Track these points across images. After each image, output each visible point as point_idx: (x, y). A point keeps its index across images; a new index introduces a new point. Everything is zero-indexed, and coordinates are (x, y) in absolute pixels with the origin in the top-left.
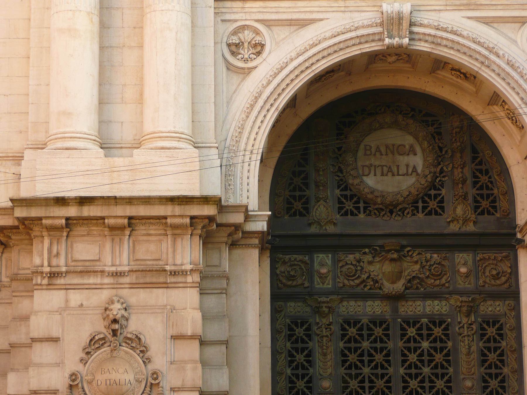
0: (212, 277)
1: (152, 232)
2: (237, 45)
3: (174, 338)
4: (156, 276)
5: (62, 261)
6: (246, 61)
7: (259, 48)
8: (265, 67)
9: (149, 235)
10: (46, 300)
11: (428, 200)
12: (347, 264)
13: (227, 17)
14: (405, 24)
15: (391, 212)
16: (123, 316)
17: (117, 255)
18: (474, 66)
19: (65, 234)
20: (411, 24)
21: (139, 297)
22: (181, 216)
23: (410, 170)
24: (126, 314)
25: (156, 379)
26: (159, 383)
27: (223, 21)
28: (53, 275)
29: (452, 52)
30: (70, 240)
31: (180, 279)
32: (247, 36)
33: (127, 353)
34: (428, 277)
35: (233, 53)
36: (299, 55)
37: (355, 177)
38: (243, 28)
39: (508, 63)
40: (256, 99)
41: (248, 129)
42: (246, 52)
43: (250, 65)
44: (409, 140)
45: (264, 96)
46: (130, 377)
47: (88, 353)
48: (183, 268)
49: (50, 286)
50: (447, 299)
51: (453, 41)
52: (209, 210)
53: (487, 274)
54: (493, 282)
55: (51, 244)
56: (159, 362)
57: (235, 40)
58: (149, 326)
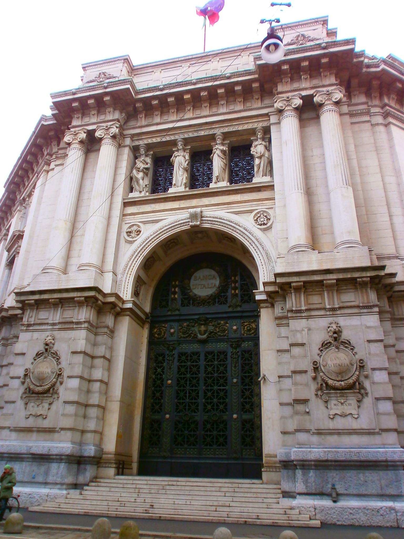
0: (101, 327)
1: (71, 305)
2: (130, 232)
3: (73, 353)
4: (68, 325)
5: (33, 319)
6: (133, 238)
7: (139, 232)
8: (140, 239)
9: (70, 307)
10: (24, 336)
11: (219, 297)
12: (183, 327)
13: (127, 222)
14: (199, 216)
15: (204, 304)
16: (51, 342)
17: (55, 316)
18: (230, 231)
19: (36, 307)
20: (202, 217)
21: (57, 334)
22: (80, 297)
23: (213, 285)
24: (53, 342)
25: (60, 371)
26: (61, 374)
27: (126, 223)
28: (29, 325)
29: (220, 227)
30: (38, 310)
31: (79, 326)
32: (135, 228)
33: (51, 359)
34: (219, 332)
35: (128, 236)
36: (154, 234)
37: (189, 289)
38: (133, 225)
39: (244, 229)
40: (135, 252)
41: (129, 265)
42: (133, 235)
43: (134, 239)
44: (213, 273)
45: (138, 251)
46: (49, 370)
47: (35, 360)
48: (81, 320)
49: (27, 331)
50: (227, 342)
51: (220, 222)
52: (92, 293)
53: (246, 329)
54: (248, 333)
55: (30, 312)
56: (64, 364)
57: (129, 230)
58: (62, 348)
